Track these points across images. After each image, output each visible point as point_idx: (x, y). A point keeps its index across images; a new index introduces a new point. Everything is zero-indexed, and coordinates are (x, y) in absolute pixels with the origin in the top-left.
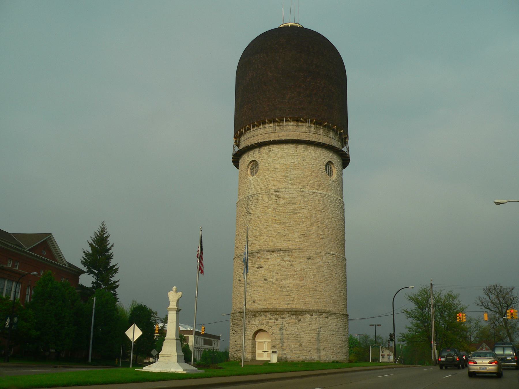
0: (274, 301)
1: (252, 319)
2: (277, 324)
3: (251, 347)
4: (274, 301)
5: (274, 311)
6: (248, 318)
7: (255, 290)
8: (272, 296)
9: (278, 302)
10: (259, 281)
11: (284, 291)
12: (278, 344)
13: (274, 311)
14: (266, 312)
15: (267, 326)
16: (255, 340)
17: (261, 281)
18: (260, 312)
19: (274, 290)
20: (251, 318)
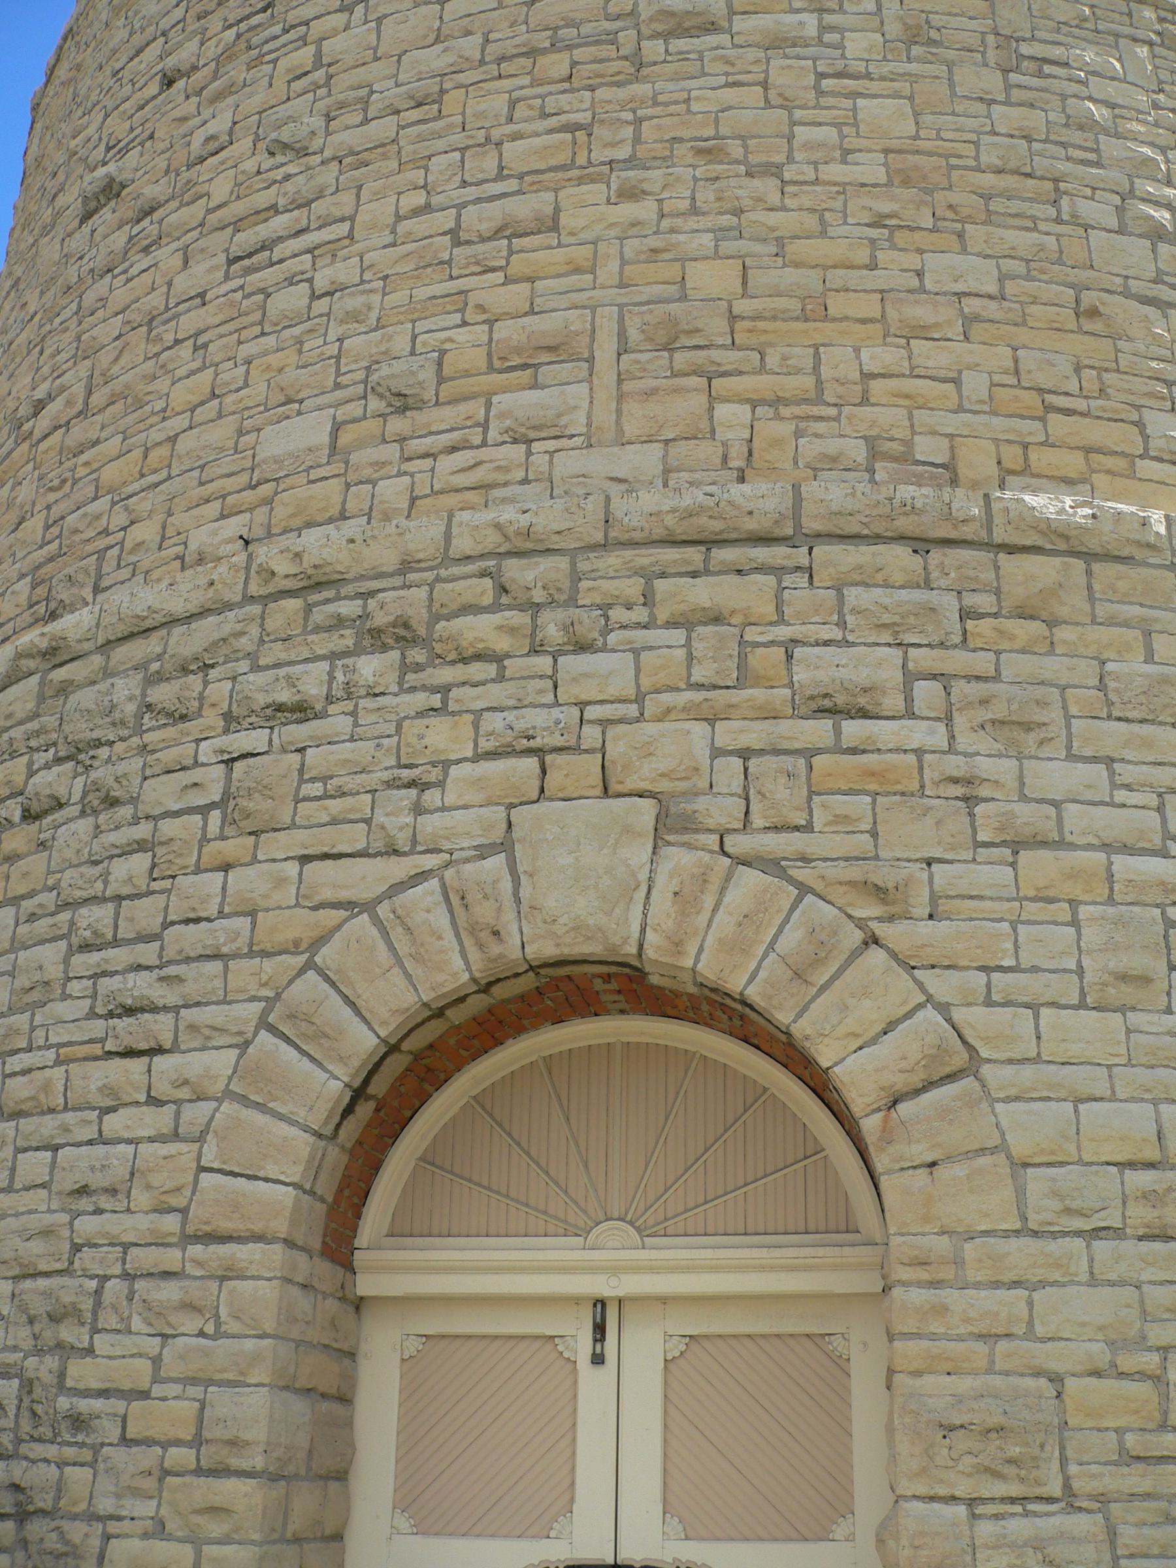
0: (877, 357)
1: (338, 723)
2: (1028, 816)
3: (258, 1434)
4: (877, 357)
5: (921, 544)
6: (212, 719)
7: (427, 208)
8: (837, 277)
9: (975, 385)
10: (532, 53)
11: (1089, 210)
12: (1099, 1352)
13: (921, 544)
14: (724, 555)
15: (750, 878)
16: (348, 1266)
17: (578, 54)
18: (553, 568)
19: (870, 169)
20: (302, 711)
